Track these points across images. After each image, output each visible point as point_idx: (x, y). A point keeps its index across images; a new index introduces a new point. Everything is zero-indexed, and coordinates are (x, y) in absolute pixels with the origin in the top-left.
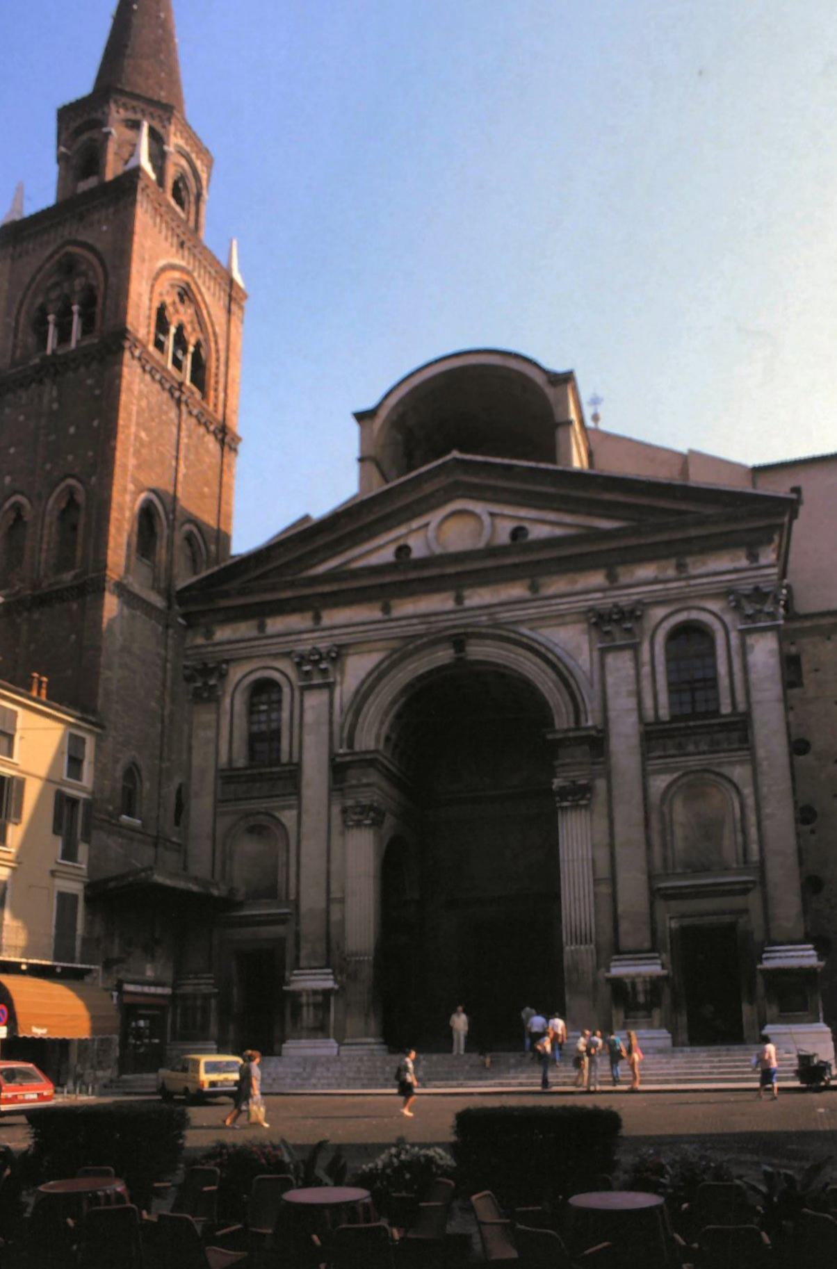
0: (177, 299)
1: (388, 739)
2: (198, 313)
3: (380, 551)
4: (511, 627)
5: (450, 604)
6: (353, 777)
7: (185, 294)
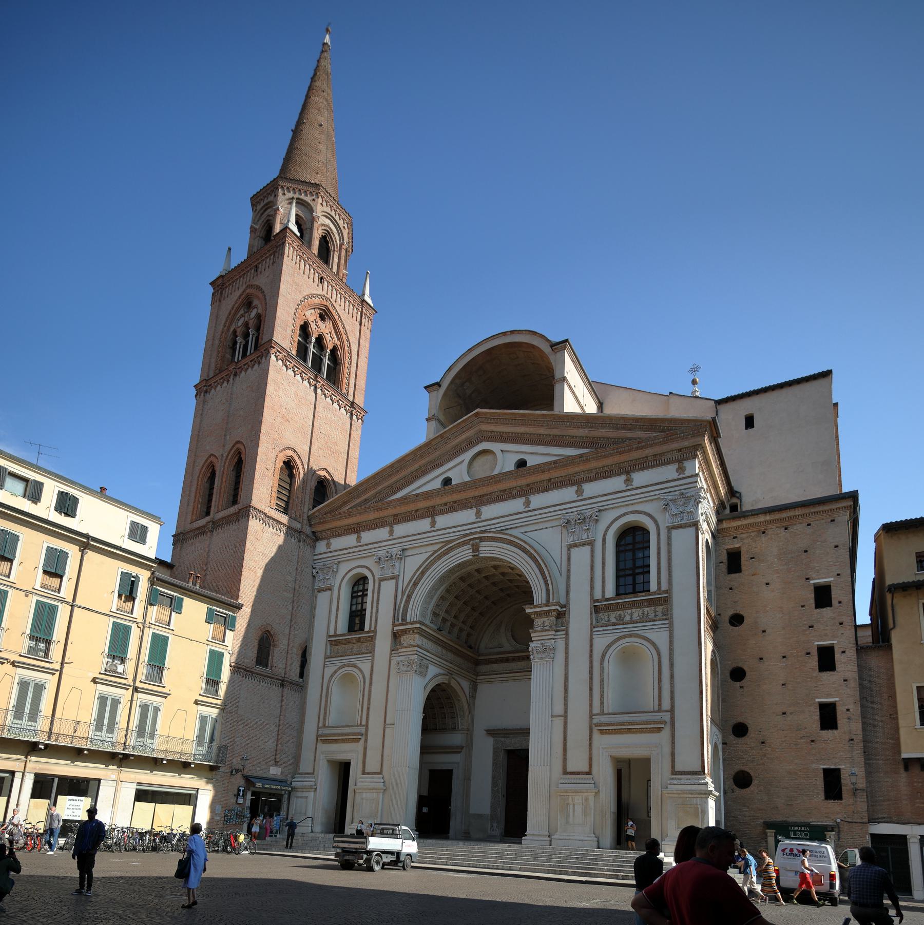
0: (319, 319)
1: (435, 614)
2: (335, 326)
3: (431, 482)
4: (506, 532)
5: (473, 518)
6: (406, 639)
7: (325, 314)
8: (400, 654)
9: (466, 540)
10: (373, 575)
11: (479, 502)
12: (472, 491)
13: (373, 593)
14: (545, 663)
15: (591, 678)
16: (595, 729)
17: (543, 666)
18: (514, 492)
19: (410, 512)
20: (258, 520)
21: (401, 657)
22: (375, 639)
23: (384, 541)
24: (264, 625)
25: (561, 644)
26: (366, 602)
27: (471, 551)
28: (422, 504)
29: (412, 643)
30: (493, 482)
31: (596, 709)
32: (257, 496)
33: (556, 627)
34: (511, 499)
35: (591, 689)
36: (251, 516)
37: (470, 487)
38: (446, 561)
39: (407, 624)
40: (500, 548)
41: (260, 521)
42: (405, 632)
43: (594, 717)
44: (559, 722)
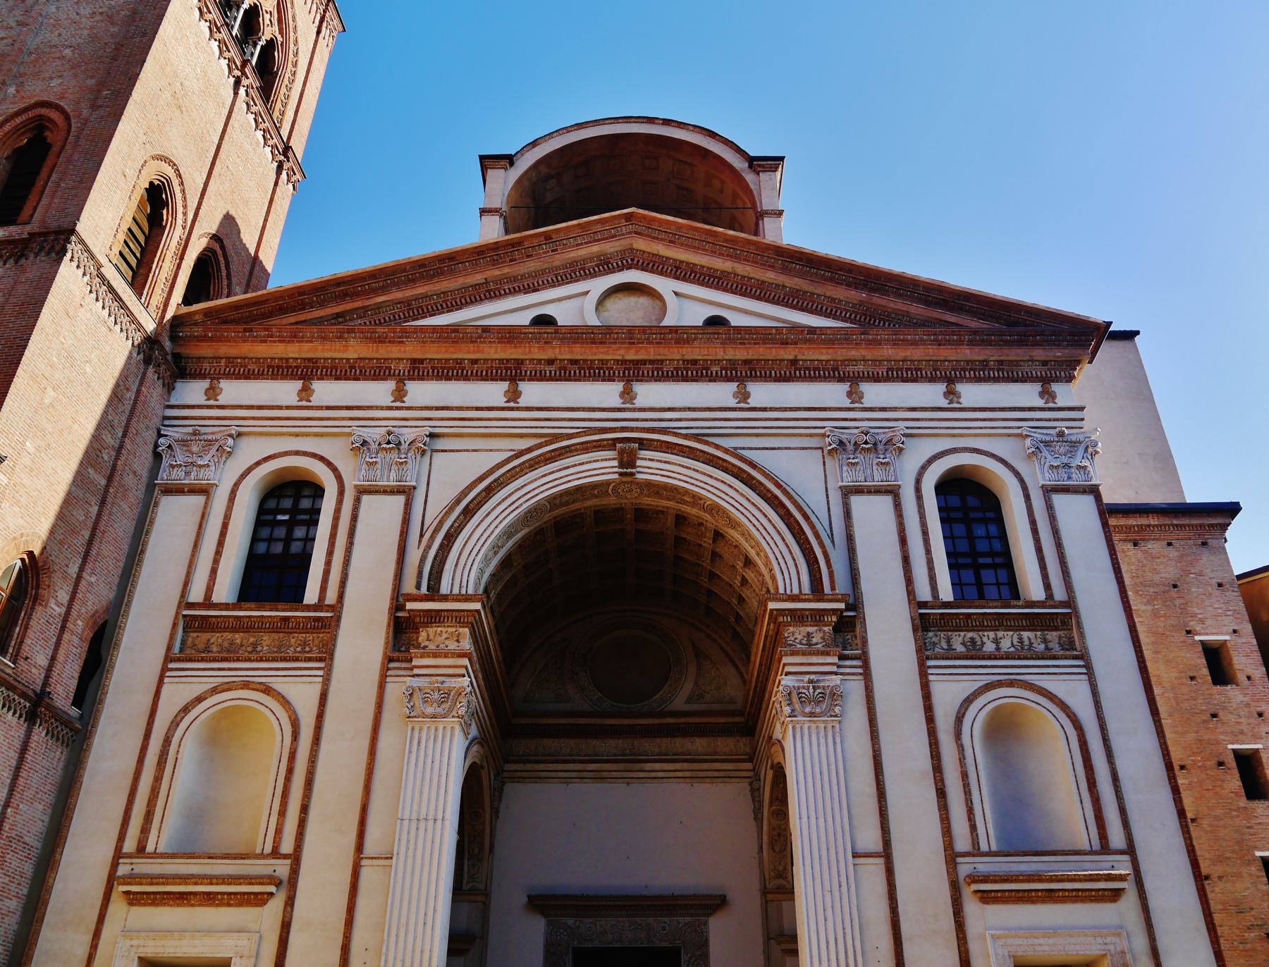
8: (416, 671)
10: (339, 478)
11: (631, 373)
12: (620, 348)
14: (822, 726)
15: (937, 768)
16: (967, 892)
17: (818, 734)
19: (459, 362)
20: (80, 271)
22: (338, 626)
23: (382, 408)
24: (28, 536)
25: (854, 688)
26: (314, 539)
27: (615, 463)
28: (495, 352)
29: (452, 646)
30: (671, 339)
31: (962, 844)
32: (91, 218)
33: (845, 648)
34: (706, 381)
35: (941, 793)
36: (69, 255)
37: (617, 338)
38: (550, 474)
39: (445, 598)
41: (84, 274)
42: (434, 618)
43: (959, 860)
44: (874, 869)
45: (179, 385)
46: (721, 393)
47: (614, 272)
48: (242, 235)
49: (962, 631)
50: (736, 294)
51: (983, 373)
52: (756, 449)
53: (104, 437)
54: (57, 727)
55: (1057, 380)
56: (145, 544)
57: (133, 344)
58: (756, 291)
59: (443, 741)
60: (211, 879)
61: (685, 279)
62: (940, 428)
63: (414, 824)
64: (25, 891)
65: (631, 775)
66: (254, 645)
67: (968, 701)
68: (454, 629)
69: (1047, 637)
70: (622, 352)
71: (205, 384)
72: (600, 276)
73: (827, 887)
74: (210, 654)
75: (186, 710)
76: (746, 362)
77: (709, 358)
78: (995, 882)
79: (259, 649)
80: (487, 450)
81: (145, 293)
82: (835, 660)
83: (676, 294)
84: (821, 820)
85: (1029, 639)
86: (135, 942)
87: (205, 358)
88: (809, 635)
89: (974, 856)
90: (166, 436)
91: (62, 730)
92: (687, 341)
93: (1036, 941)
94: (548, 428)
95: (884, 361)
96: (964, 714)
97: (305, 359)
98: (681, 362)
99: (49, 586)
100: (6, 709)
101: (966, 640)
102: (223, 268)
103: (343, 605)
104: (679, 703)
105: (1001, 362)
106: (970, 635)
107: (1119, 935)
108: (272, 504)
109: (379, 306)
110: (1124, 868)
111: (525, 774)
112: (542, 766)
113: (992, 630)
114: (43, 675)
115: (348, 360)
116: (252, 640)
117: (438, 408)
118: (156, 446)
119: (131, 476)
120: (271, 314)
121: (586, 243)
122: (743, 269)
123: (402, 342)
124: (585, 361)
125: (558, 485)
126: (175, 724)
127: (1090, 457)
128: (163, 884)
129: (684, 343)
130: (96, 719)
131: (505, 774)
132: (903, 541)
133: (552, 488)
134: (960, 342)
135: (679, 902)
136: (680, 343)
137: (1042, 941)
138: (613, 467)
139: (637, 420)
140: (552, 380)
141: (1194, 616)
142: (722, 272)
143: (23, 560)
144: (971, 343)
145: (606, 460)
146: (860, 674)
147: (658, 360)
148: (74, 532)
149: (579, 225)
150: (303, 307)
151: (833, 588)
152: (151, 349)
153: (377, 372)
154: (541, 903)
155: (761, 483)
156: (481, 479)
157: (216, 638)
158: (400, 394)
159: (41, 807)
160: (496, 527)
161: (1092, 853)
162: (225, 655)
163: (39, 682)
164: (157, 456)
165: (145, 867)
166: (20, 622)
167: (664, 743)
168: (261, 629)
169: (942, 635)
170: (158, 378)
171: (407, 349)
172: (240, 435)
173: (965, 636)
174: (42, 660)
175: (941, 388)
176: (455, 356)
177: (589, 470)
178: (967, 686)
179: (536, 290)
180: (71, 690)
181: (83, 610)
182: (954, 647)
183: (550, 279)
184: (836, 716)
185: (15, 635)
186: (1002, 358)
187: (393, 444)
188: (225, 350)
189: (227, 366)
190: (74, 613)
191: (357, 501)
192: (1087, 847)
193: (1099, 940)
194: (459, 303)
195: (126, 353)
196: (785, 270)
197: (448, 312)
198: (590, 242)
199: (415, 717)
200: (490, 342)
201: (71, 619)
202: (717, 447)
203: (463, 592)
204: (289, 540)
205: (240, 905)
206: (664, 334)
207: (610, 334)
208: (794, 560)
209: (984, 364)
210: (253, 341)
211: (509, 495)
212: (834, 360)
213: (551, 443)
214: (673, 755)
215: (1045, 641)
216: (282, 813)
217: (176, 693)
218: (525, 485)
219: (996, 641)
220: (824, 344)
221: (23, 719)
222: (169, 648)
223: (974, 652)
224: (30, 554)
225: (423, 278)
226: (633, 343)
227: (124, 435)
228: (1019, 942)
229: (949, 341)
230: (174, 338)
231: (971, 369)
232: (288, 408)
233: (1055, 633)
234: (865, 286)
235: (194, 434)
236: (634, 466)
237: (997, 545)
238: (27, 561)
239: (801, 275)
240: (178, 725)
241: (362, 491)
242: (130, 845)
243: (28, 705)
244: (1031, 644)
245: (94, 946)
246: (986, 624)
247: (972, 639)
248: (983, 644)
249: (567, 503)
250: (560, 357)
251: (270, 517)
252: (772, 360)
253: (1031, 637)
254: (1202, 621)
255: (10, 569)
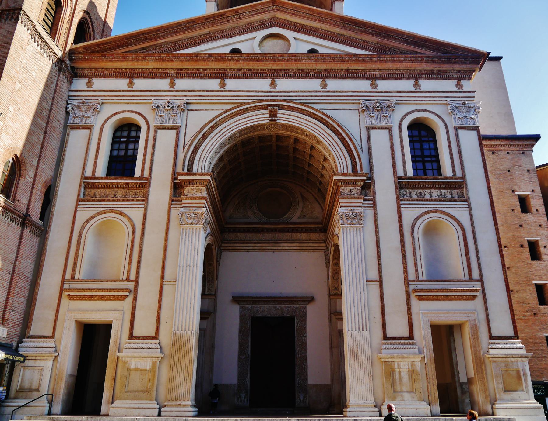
8: (183, 205)
9: (263, 105)
12: (270, 63)
13: (147, 140)
14: (355, 228)
15: (403, 246)
16: (413, 296)
17: (353, 232)
18: (312, 73)
19: (198, 70)
20: (26, 28)
21: (184, 208)
22: (150, 186)
23: (165, 91)
25: (369, 213)
26: (137, 149)
27: (268, 116)
28: (214, 65)
29: (199, 194)
30: (293, 59)
31: (412, 276)
33: (366, 196)
34: (308, 79)
35: (404, 256)
36: (20, 20)
37: (269, 59)
38: (239, 120)
39: (195, 174)
40: (300, 118)
41: (28, 30)
42: (190, 183)
43: (410, 283)
45: (75, 81)
46: (314, 84)
47: (267, 28)
48: (98, 11)
49: (416, 189)
50: (322, 38)
51: (431, 76)
52: (329, 109)
53: (43, 104)
54: (34, 229)
55: (464, 79)
56: (65, 151)
57: (53, 62)
58: (331, 37)
59: (196, 234)
60: (102, 290)
61: (299, 32)
62: (411, 100)
63: (185, 268)
64: (27, 295)
65: (275, 248)
66: (115, 195)
67: (417, 219)
68: (199, 188)
69: (452, 192)
70: (271, 65)
71: (86, 80)
72: (260, 30)
73: (355, 294)
74: (96, 198)
75: (87, 221)
76: (326, 70)
77: (310, 68)
78: (424, 292)
79: (117, 196)
80: (211, 110)
81: (56, 38)
82: (362, 201)
83: (295, 38)
84: (354, 267)
85: (445, 193)
86: (73, 314)
87: (85, 68)
88: (351, 190)
89: (416, 281)
90: (71, 104)
91: (36, 230)
92: (300, 61)
93: (440, 315)
94: (238, 100)
95: (387, 70)
96: (415, 224)
97: (130, 69)
98: (297, 70)
99: (25, 170)
100: (12, 221)
101: (418, 193)
102: (91, 27)
103: (151, 178)
104: (295, 219)
105: (439, 71)
106: (419, 191)
107: (474, 313)
108: (118, 134)
109: (161, 45)
110: (478, 286)
111: (230, 248)
112: (238, 245)
113: (429, 189)
114: (26, 207)
115: (149, 69)
116: (113, 192)
117: (189, 91)
118: (66, 108)
119: (57, 122)
120: (113, 48)
121: (254, 14)
122: (325, 27)
123: (173, 61)
124: (254, 69)
125: (243, 125)
126: (83, 227)
127: (476, 114)
128: (83, 292)
129: (298, 61)
130: (50, 226)
131: (222, 248)
132: (393, 150)
133: (240, 126)
134: (422, 61)
135: (295, 299)
136: (296, 61)
137: (442, 315)
138: (267, 117)
139: (277, 96)
140: (240, 78)
141: (516, 184)
142: (316, 28)
143: (13, 159)
144: (427, 62)
145: (264, 114)
146: (372, 207)
147: (287, 69)
148: (34, 146)
149: (251, 6)
150: (127, 45)
151: (361, 170)
152: (61, 64)
153: (162, 74)
154: (238, 299)
155: (331, 125)
156: (209, 122)
157: (98, 192)
158: (172, 85)
159: (30, 261)
160: (216, 144)
161: (465, 281)
162: (102, 199)
163: (25, 210)
164: (67, 113)
165: (74, 285)
166: (14, 185)
167: (289, 235)
168: (117, 188)
169: (408, 191)
170: (65, 78)
171: (175, 64)
172: (103, 103)
173: (417, 191)
174: (25, 201)
175: (412, 82)
176: (196, 67)
177: (256, 119)
178: (418, 212)
179: (231, 37)
180: (38, 213)
181: (41, 180)
182: (412, 196)
183: (238, 32)
184: (361, 224)
185: (13, 191)
186: (440, 69)
187: (170, 107)
188: (94, 65)
189: (95, 72)
190: (37, 181)
191: (156, 132)
192: (464, 279)
193: (466, 315)
194: (197, 43)
195: (50, 66)
196: (344, 27)
197: (193, 47)
198: (256, 14)
199: (184, 224)
200: (212, 61)
201: (36, 184)
202: (313, 108)
203: (203, 172)
204: (127, 149)
205: (115, 300)
206: (289, 57)
207: (265, 57)
208: (345, 158)
209: (432, 71)
210: (106, 61)
211: (222, 130)
212: (365, 69)
213: (238, 107)
214: (293, 240)
215: (451, 194)
216: (130, 263)
217: (83, 215)
218: (229, 125)
219: (431, 194)
220: (361, 62)
221: (19, 226)
222: (78, 196)
223: (421, 198)
224: (16, 156)
225: (181, 31)
226: (276, 61)
227: (52, 104)
228: (433, 315)
229: (417, 61)
230: (71, 59)
231: (426, 74)
232: (123, 91)
233: (456, 190)
234: (380, 35)
235: (83, 103)
236: (276, 117)
237: (433, 153)
238: (15, 159)
239: (351, 29)
240: (84, 228)
241: (157, 128)
242: (68, 277)
243: (21, 220)
244: (445, 195)
245: (57, 316)
246: (426, 186)
247: (420, 193)
248: (425, 194)
249: (247, 133)
250: (243, 68)
251: (118, 140)
252: (338, 69)
253: (446, 192)
254: (519, 186)
255: (7, 163)
